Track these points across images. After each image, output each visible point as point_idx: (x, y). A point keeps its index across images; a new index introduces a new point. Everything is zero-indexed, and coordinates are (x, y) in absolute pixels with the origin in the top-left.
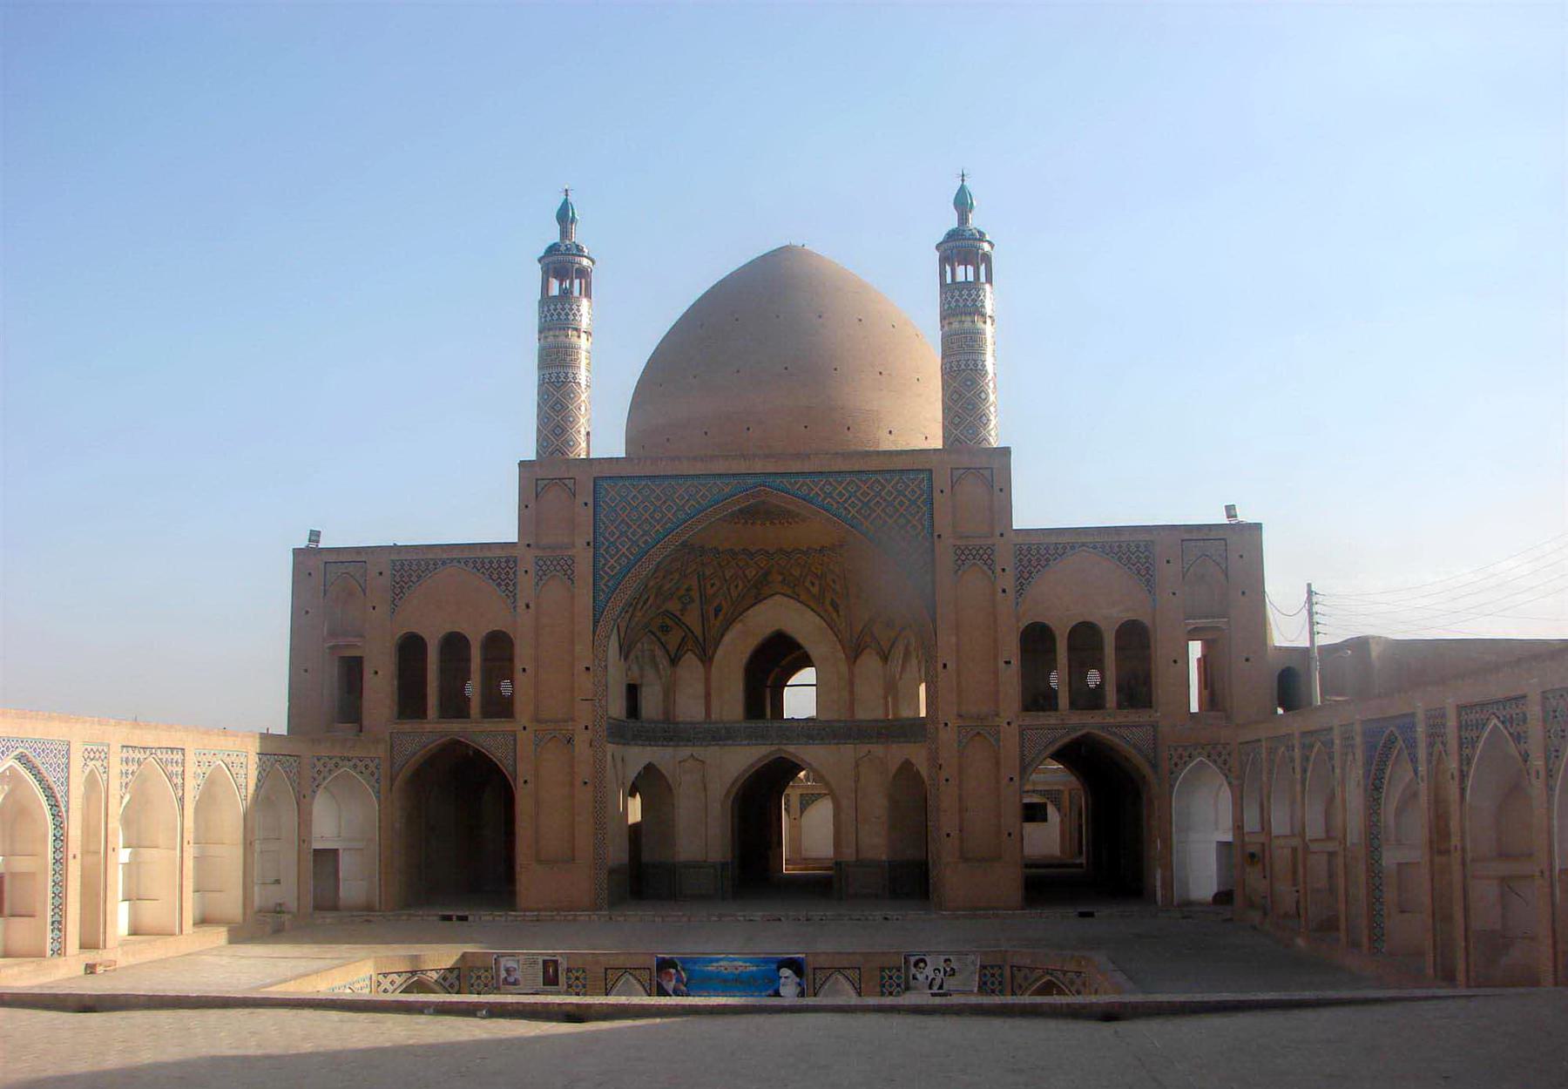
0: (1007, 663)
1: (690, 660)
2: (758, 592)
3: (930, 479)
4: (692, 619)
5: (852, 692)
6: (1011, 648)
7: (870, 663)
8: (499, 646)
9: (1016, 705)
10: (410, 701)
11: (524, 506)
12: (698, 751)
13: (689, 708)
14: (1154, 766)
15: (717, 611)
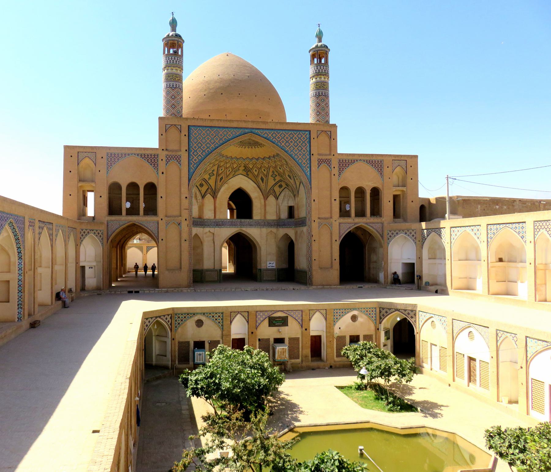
0: (335, 200)
1: (209, 197)
2: (235, 173)
3: (310, 134)
4: (212, 182)
5: (265, 210)
6: (336, 195)
7: (271, 199)
8: (151, 188)
9: (338, 215)
10: (114, 209)
11: (161, 135)
12: (212, 230)
13: (208, 214)
14: (382, 237)
15: (221, 179)
